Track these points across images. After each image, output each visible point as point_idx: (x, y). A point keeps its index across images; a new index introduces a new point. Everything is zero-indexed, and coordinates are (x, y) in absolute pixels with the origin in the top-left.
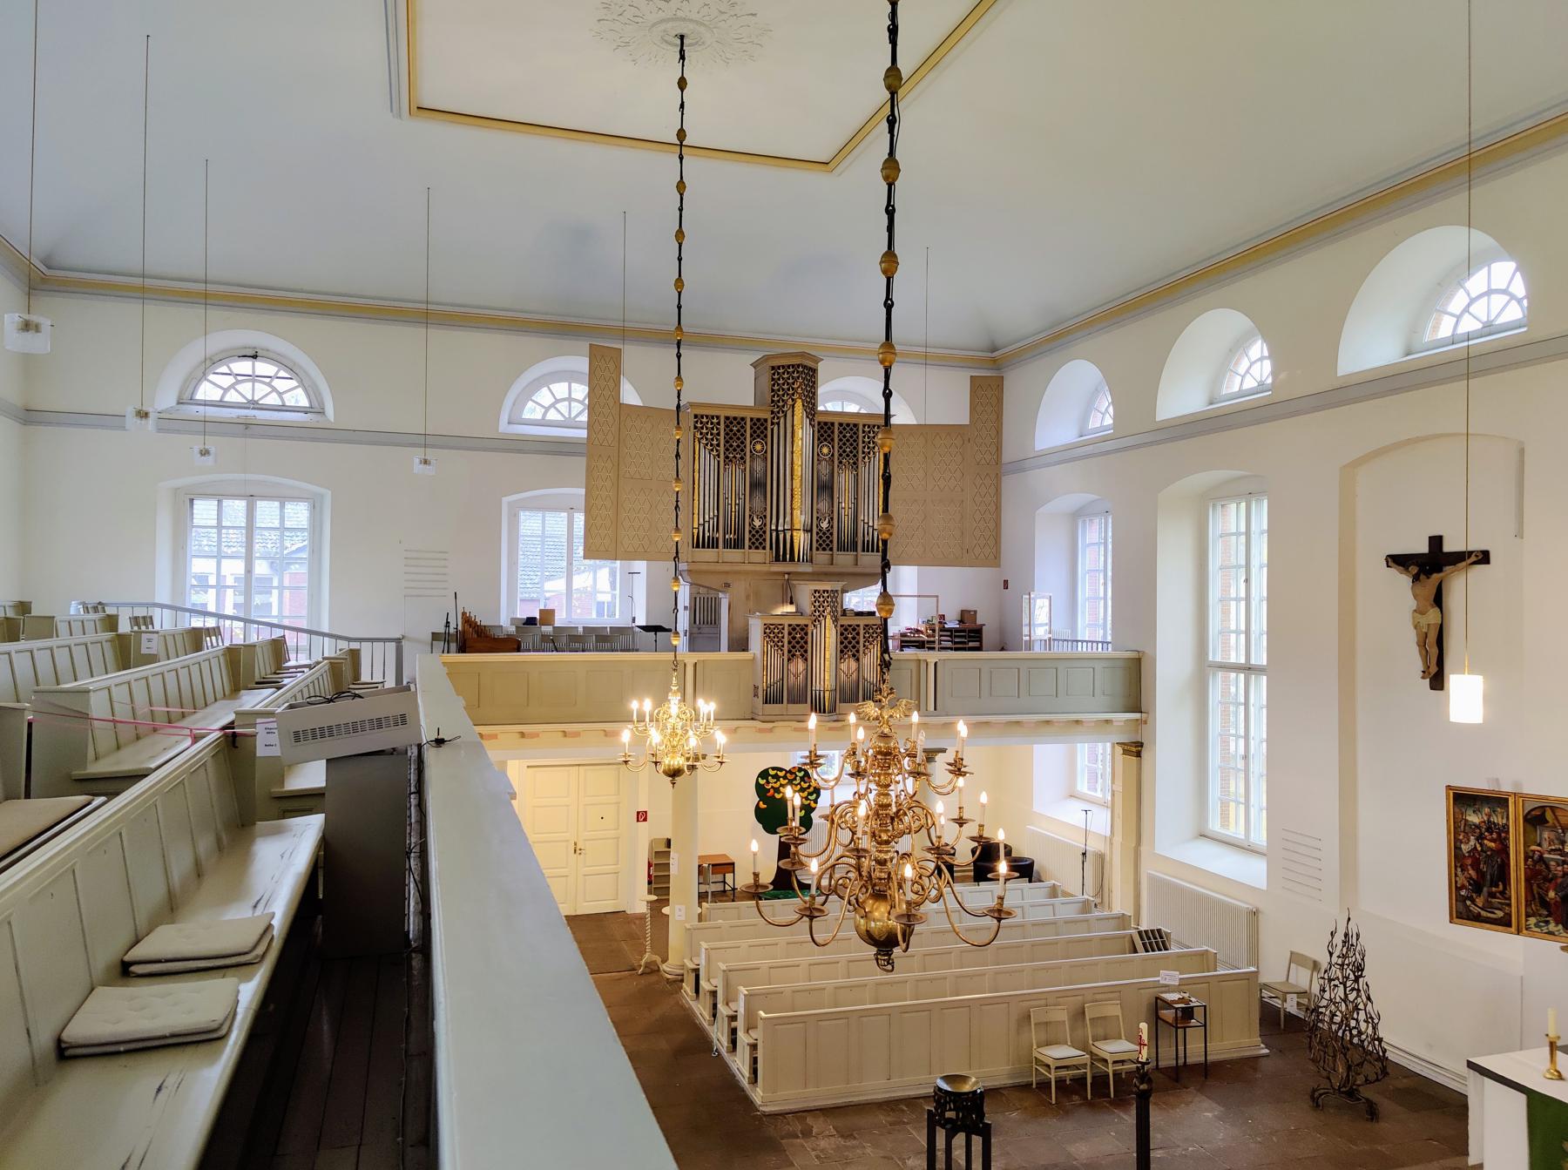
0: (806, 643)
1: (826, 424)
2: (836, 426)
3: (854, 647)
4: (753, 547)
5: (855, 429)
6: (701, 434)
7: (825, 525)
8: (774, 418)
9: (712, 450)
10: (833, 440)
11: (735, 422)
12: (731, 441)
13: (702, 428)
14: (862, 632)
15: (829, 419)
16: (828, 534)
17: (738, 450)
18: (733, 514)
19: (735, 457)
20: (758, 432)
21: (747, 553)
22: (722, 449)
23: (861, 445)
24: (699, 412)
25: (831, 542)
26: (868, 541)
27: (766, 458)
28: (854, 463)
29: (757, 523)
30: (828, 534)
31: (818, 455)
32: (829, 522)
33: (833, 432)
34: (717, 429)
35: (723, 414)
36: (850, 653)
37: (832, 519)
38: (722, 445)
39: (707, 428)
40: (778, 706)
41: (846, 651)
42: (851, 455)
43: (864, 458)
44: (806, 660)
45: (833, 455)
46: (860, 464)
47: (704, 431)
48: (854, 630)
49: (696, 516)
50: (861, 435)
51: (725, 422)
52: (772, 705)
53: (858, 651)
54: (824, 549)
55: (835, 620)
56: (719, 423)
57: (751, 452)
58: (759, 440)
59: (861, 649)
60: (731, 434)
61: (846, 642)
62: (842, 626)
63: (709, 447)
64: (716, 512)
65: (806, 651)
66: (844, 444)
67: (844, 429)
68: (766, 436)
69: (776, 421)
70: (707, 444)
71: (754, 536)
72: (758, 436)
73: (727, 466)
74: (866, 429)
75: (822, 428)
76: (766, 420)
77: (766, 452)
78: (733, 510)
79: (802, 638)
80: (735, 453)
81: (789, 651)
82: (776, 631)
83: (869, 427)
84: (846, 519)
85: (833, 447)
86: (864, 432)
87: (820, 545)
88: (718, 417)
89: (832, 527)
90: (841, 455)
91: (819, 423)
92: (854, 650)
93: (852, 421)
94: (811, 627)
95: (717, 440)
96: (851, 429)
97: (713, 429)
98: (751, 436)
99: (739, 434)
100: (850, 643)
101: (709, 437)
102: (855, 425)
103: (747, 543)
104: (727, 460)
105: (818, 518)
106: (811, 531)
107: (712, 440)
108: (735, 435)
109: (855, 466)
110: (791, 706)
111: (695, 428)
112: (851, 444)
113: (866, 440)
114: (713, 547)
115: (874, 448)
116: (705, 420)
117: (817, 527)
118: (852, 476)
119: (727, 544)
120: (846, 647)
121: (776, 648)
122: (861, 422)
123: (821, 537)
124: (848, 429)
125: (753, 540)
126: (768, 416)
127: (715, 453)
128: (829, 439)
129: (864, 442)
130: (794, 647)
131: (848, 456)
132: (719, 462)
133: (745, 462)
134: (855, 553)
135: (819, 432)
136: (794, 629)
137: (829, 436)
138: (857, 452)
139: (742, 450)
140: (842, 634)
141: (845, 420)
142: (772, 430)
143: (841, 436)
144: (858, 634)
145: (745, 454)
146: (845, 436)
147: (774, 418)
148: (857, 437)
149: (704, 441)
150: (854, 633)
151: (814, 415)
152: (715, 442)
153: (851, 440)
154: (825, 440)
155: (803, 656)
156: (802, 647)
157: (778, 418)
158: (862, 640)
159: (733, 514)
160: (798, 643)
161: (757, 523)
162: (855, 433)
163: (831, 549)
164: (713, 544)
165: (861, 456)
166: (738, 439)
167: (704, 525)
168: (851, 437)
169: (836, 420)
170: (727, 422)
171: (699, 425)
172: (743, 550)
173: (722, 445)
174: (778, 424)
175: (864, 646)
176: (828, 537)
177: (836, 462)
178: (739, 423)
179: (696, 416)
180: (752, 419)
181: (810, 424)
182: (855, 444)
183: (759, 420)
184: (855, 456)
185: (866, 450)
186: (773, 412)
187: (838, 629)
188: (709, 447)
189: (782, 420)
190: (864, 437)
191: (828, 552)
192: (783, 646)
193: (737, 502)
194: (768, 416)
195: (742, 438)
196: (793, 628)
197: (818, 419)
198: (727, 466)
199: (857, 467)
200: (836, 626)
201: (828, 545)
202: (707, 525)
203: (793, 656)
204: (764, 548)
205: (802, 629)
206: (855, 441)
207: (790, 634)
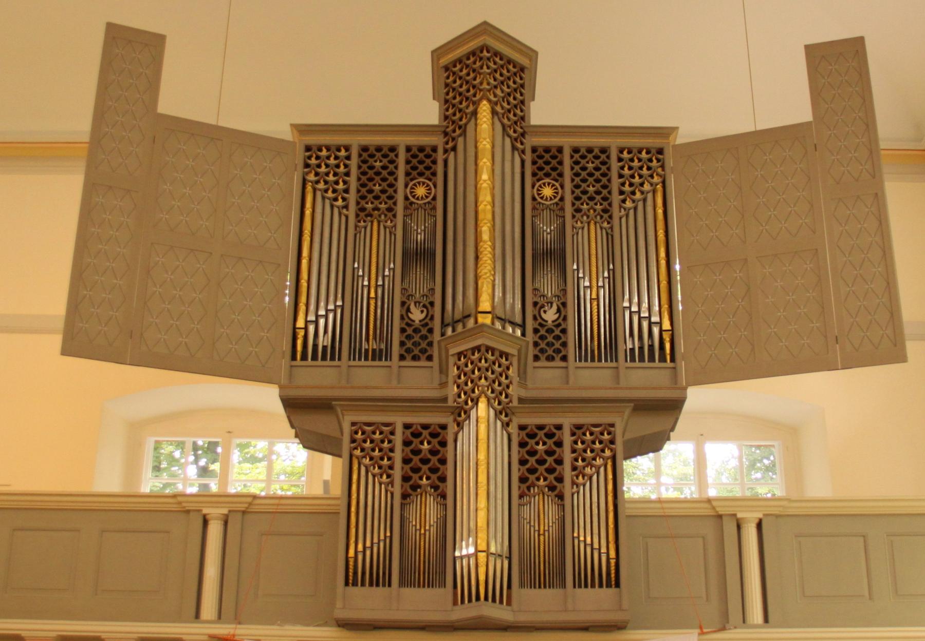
0: (443, 461)
1: (547, 150)
2: (567, 152)
3: (550, 471)
4: (409, 357)
5: (603, 157)
6: (317, 174)
7: (550, 316)
8: (447, 143)
9: (336, 199)
10: (561, 175)
11: (378, 155)
12: (371, 184)
13: (319, 166)
14: (567, 440)
15: (553, 141)
16: (557, 332)
17: (384, 196)
18: (372, 302)
19: (378, 209)
20: (421, 167)
21: (395, 369)
22: (352, 197)
23: (616, 182)
24: (313, 140)
25: (564, 344)
26: (651, 347)
27: (434, 208)
28: (605, 211)
29: (417, 315)
30: (557, 332)
31: (534, 199)
32: (559, 311)
33: (561, 163)
34: (346, 166)
35: (356, 141)
36: (541, 482)
37: (564, 305)
38: (353, 190)
39: (327, 166)
40: (380, 591)
41: (532, 478)
42: (598, 198)
43: (624, 201)
44: (444, 496)
45: (562, 199)
46: (616, 212)
47: (323, 169)
48: (550, 435)
49: (302, 307)
50: (615, 165)
51: (360, 155)
52: (367, 589)
53: (560, 479)
54: (550, 358)
55: (504, 412)
56: (348, 158)
57: (406, 198)
58: (421, 180)
59: (568, 474)
60: (371, 173)
61: (532, 460)
62: (522, 428)
63: (330, 194)
64: (339, 303)
65: (443, 479)
66: (584, 181)
67: (583, 157)
68: (434, 174)
69: (451, 145)
70: (326, 191)
71: (409, 337)
72: (421, 174)
73: (362, 224)
74: (625, 155)
75: (541, 157)
76: (434, 149)
77: (434, 199)
78: (372, 295)
79: (434, 452)
80: (376, 202)
81: (406, 479)
82: (377, 436)
83: (629, 152)
84: (595, 307)
85: (562, 187)
86: (620, 160)
87: (542, 351)
88: (347, 149)
89: (565, 319)
90: (578, 198)
91: (534, 150)
92: (551, 477)
93: (597, 142)
94: (452, 428)
95: (345, 182)
96: (596, 157)
97: (338, 166)
98: (407, 174)
99: (384, 173)
100: (541, 462)
101: (331, 178)
102: (604, 150)
103: (396, 349)
104: (362, 214)
105: (535, 304)
106: (523, 326)
107: (337, 183)
108: (377, 174)
109: (606, 216)
110: (407, 591)
111: (307, 166)
112: (598, 181)
113: (626, 171)
114: (333, 358)
115: (642, 185)
116: (324, 153)
117: (535, 318)
118: (602, 237)
119: (357, 353)
120: (532, 471)
121: (377, 470)
122: (613, 143)
123: (542, 338)
124: (590, 156)
125: (409, 344)
126: (437, 140)
127: (340, 202)
128: (554, 174)
129: (621, 176)
130: (416, 470)
131: (591, 199)
132: (347, 217)
133: (395, 216)
134: (614, 364)
135: (534, 163)
136: (416, 435)
137: (554, 169)
138: (610, 193)
139: (390, 197)
140: (522, 445)
141: (583, 141)
142: (446, 162)
143: (577, 168)
144: (559, 444)
145: (395, 204)
146: (584, 169)
147: (447, 143)
148: (609, 169)
149: (321, 186)
150: (550, 442)
151: (523, 135)
152: (341, 186)
153: (597, 174)
154: (547, 175)
155: (436, 488)
156: (434, 470)
157: (453, 139)
158: (568, 457)
159: (372, 302)
160: (425, 461)
161: (417, 315)
162: (603, 163)
163: (564, 358)
164: (331, 353)
165: (616, 198)
166: (384, 180)
167: (316, 323)
168: (597, 169)
169: (567, 142)
170: (365, 155)
171: (313, 161)
172: (388, 363)
173: (353, 190)
174: (454, 149)
175: (574, 468)
176: (557, 338)
177: (569, 210)
178: (385, 156)
179: (308, 148)
180: (408, 149)
181: (514, 148)
182: (604, 180)
183: (421, 149)
184: (605, 199)
185: (627, 188)
186: (446, 134)
187: (513, 429)
188: (330, 194)
189: (461, 140)
190: (622, 168)
191: (558, 363)
192: (391, 467)
193: (380, 283)
194: (437, 140)
195: (391, 179)
196: (414, 433)
197: (532, 141)
198: (362, 224)
199: (611, 217)
200: (506, 425)
201: (558, 351)
202: (322, 322)
203: (415, 487)
204: (430, 358)
205: (434, 435)
206: (604, 175)
207: (406, 443)
